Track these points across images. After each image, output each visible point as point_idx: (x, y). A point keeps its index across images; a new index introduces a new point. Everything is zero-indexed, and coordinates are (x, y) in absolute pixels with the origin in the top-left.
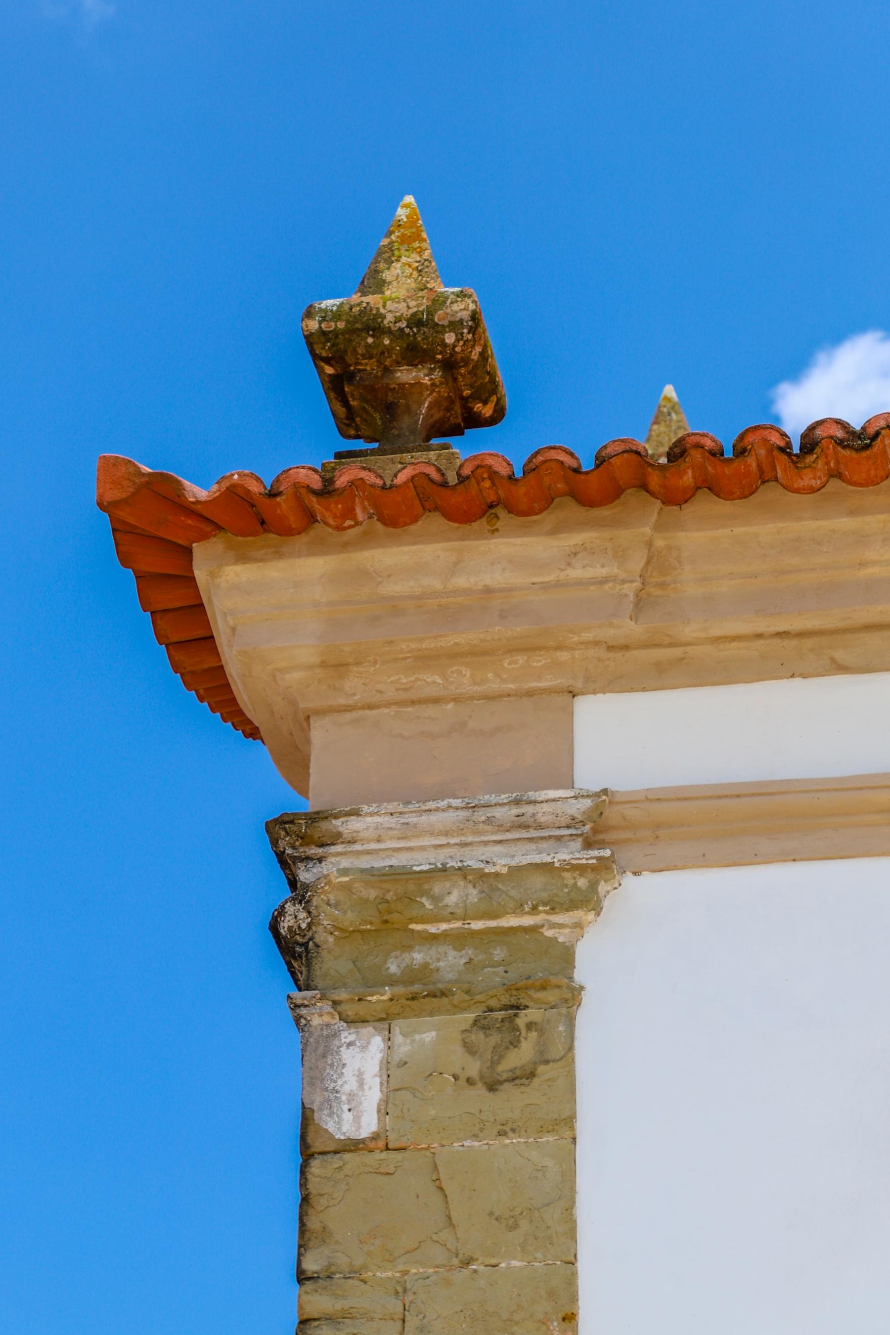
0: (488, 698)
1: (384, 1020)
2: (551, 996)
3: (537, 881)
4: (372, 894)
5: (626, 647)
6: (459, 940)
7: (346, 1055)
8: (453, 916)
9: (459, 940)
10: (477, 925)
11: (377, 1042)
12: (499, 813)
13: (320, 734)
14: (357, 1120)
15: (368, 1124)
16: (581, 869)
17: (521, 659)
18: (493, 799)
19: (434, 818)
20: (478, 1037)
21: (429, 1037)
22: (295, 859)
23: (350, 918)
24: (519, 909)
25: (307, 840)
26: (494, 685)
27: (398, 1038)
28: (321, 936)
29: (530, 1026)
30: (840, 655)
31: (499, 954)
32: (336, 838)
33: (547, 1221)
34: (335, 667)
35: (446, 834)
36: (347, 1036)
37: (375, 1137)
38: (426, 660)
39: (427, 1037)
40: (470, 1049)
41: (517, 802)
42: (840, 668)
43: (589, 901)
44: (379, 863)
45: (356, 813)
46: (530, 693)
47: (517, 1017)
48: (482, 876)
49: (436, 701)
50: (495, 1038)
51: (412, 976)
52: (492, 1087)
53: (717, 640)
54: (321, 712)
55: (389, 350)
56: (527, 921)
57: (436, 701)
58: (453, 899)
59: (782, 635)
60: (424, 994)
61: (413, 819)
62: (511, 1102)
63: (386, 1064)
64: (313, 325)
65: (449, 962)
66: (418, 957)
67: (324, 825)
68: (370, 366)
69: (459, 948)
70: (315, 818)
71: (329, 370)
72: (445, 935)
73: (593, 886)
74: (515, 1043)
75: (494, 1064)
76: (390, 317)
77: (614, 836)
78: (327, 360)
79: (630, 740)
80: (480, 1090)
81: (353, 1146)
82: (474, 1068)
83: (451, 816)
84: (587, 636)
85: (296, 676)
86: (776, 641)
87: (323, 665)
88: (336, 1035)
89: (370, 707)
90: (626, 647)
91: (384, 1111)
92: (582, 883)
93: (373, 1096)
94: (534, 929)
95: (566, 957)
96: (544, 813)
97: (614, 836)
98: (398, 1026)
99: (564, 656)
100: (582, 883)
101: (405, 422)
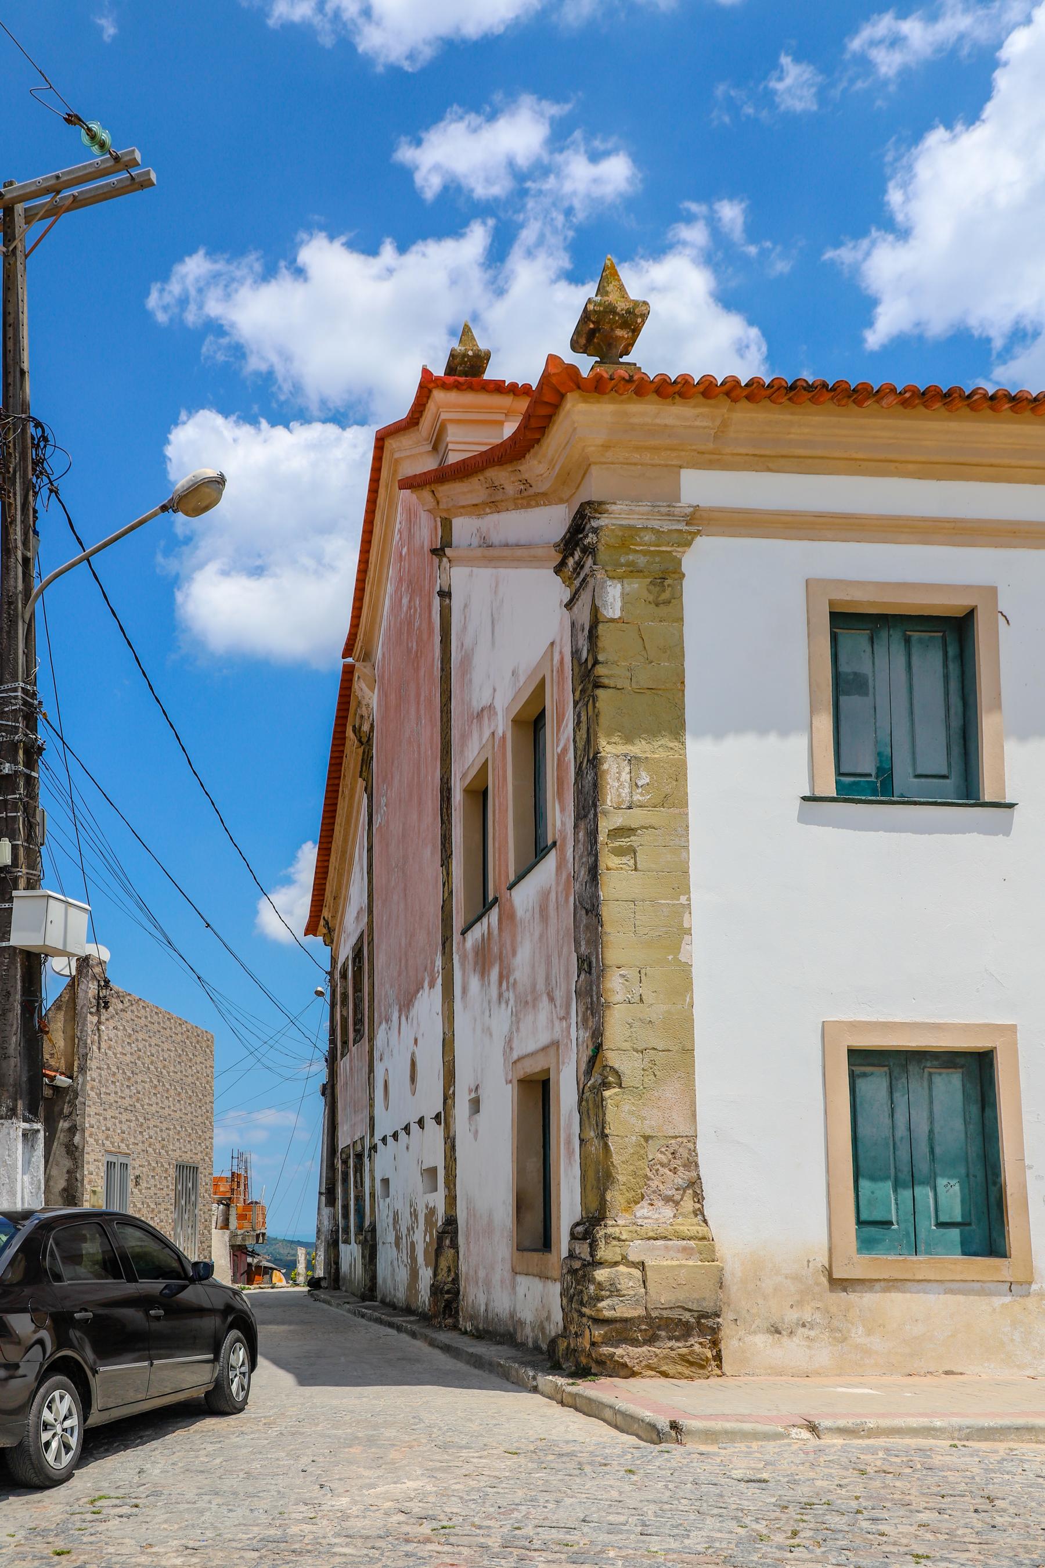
0: (653, 465)
1: (621, 578)
2: (676, 576)
3: (675, 535)
4: (620, 534)
5: (703, 453)
6: (645, 553)
7: (609, 589)
8: (646, 545)
9: (645, 553)
10: (652, 549)
11: (619, 586)
12: (662, 509)
13: (594, 470)
14: (614, 612)
15: (617, 614)
16: (690, 533)
17: (669, 452)
18: (661, 504)
19: (641, 508)
20: (652, 587)
21: (636, 586)
22: (590, 518)
23: (612, 541)
24: (668, 545)
25: (596, 511)
26: (657, 461)
27: (626, 586)
28: (600, 546)
29: (669, 586)
30: (770, 465)
31: (657, 559)
32: (606, 511)
33: (674, 651)
34: (606, 447)
35: (643, 514)
36: (609, 583)
37: (620, 618)
38: (637, 449)
39: (635, 585)
40: (649, 591)
41: (669, 506)
42: (769, 470)
43: (689, 544)
44: (623, 522)
45: (615, 503)
46: (667, 466)
47: (664, 582)
48: (658, 531)
49: (635, 464)
50: (658, 589)
51: (629, 564)
52: (657, 605)
53: (733, 454)
54: (595, 463)
55: (617, 321)
56: (669, 549)
57: (635, 464)
58: (646, 538)
59: (754, 455)
60: (634, 571)
61: (633, 508)
62: (663, 610)
63: (622, 594)
64: (591, 307)
65: (642, 561)
66: (631, 557)
67: (603, 507)
68: (607, 327)
69: (644, 555)
70: (600, 503)
71: (592, 326)
72: (641, 551)
73: (693, 539)
74: (664, 591)
75: (658, 597)
76: (619, 309)
77: (699, 521)
78: (593, 322)
79: (700, 487)
80: (653, 606)
81: (612, 620)
82: (651, 598)
83: (646, 508)
84: (694, 447)
85: (593, 448)
86: (752, 458)
87: (602, 446)
88: (605, 582)
89: (613, 463)
90: (703, 453)
91: (622, 610)
92: (689, 538)
93: (618, 604)
94: (670, 552)
95: (680, 561)
96: (677, 511)
97: (699, 521)
98: (626, 581)
99: (683, 453)
100: (689, 538)
101: (614, 351)
